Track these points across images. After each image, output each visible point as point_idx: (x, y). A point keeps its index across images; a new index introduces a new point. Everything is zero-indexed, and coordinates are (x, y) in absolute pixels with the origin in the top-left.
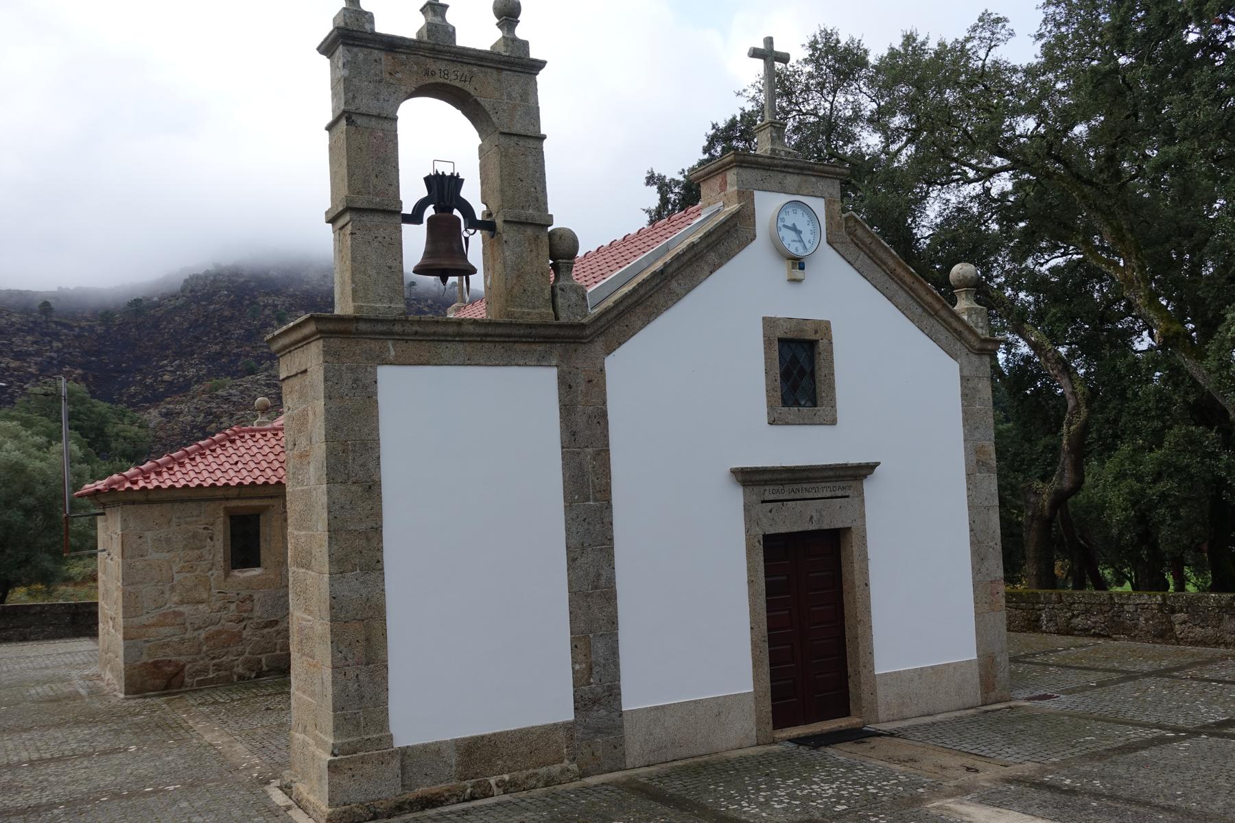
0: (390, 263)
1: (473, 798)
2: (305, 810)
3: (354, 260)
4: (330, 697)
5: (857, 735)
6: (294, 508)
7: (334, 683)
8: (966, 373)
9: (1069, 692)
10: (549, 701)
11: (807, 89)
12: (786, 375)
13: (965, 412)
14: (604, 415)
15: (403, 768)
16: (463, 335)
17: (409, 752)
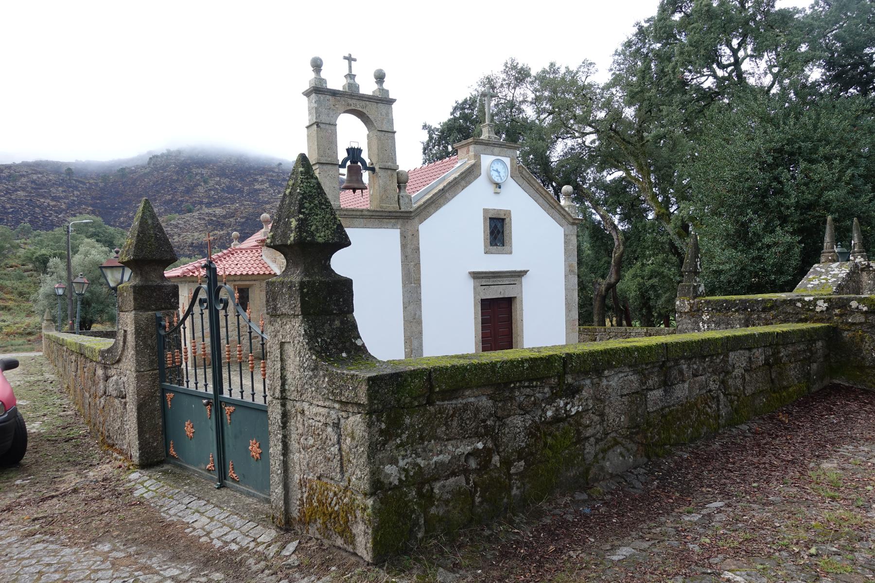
12: (492, 233)
14: (418, 249)
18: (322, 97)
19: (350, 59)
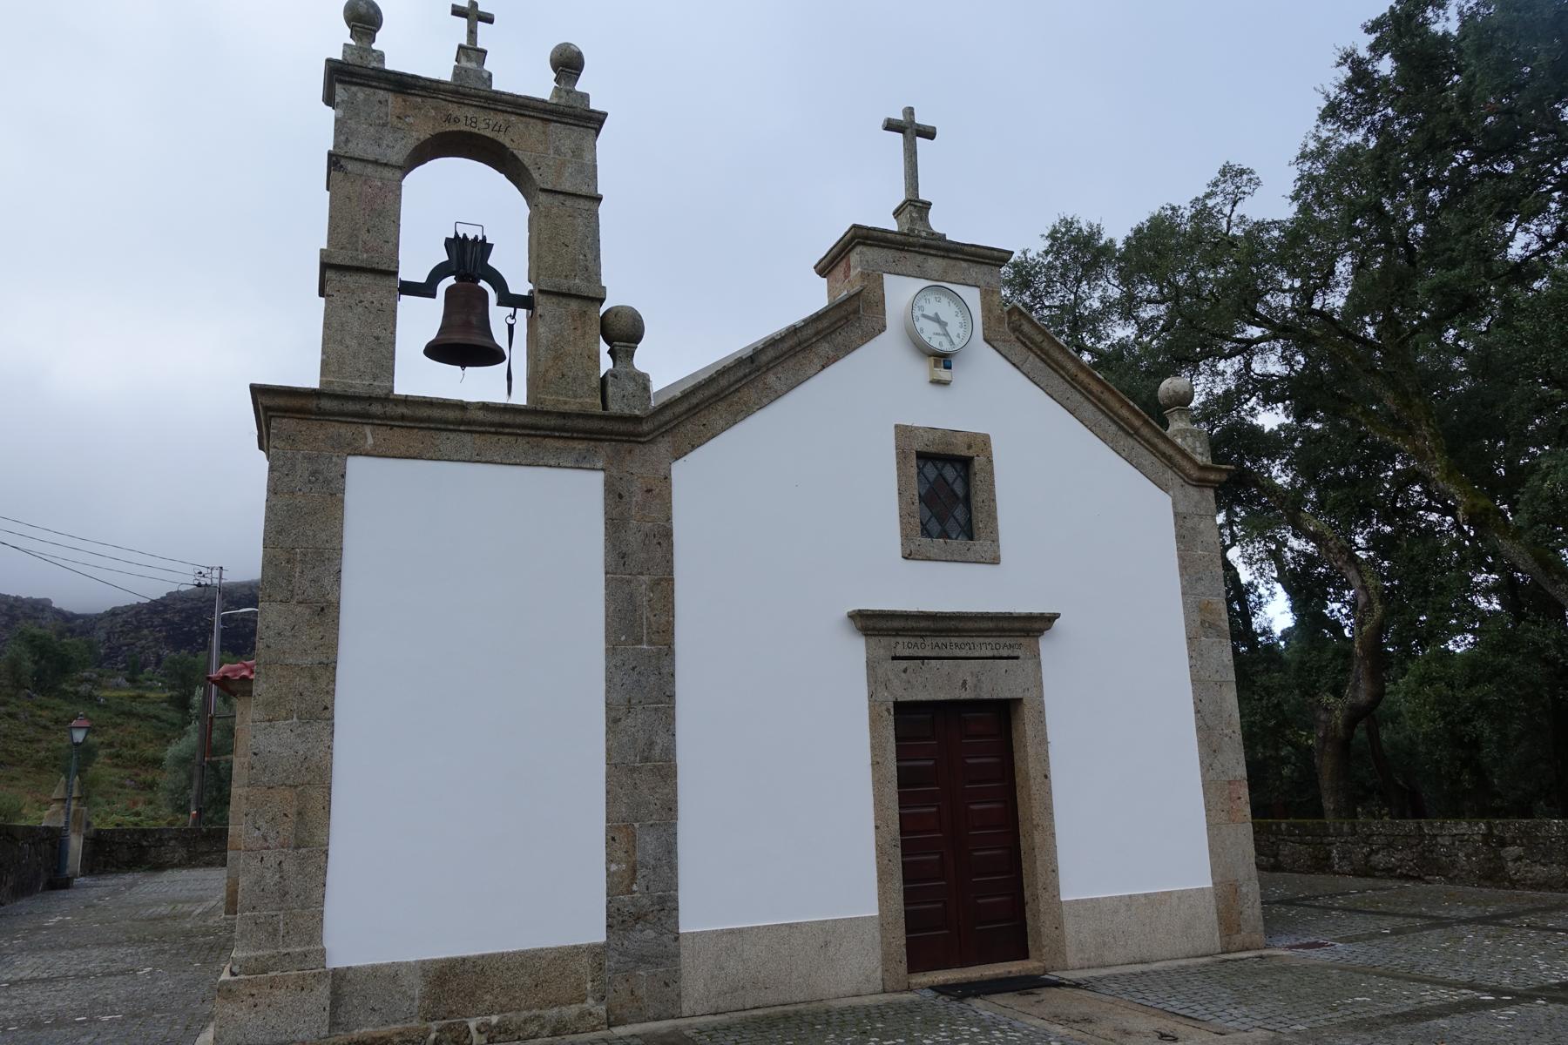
0: (377, 332)
5: (1028, 985)
8: (1181, 509)
9: (1348, 940)
10: (567, 909)
13: (1181, 558)
14: (668, 534)
16: (469, 423)
17: (350, 975)
18: (361, 94)
19: (473, 15)
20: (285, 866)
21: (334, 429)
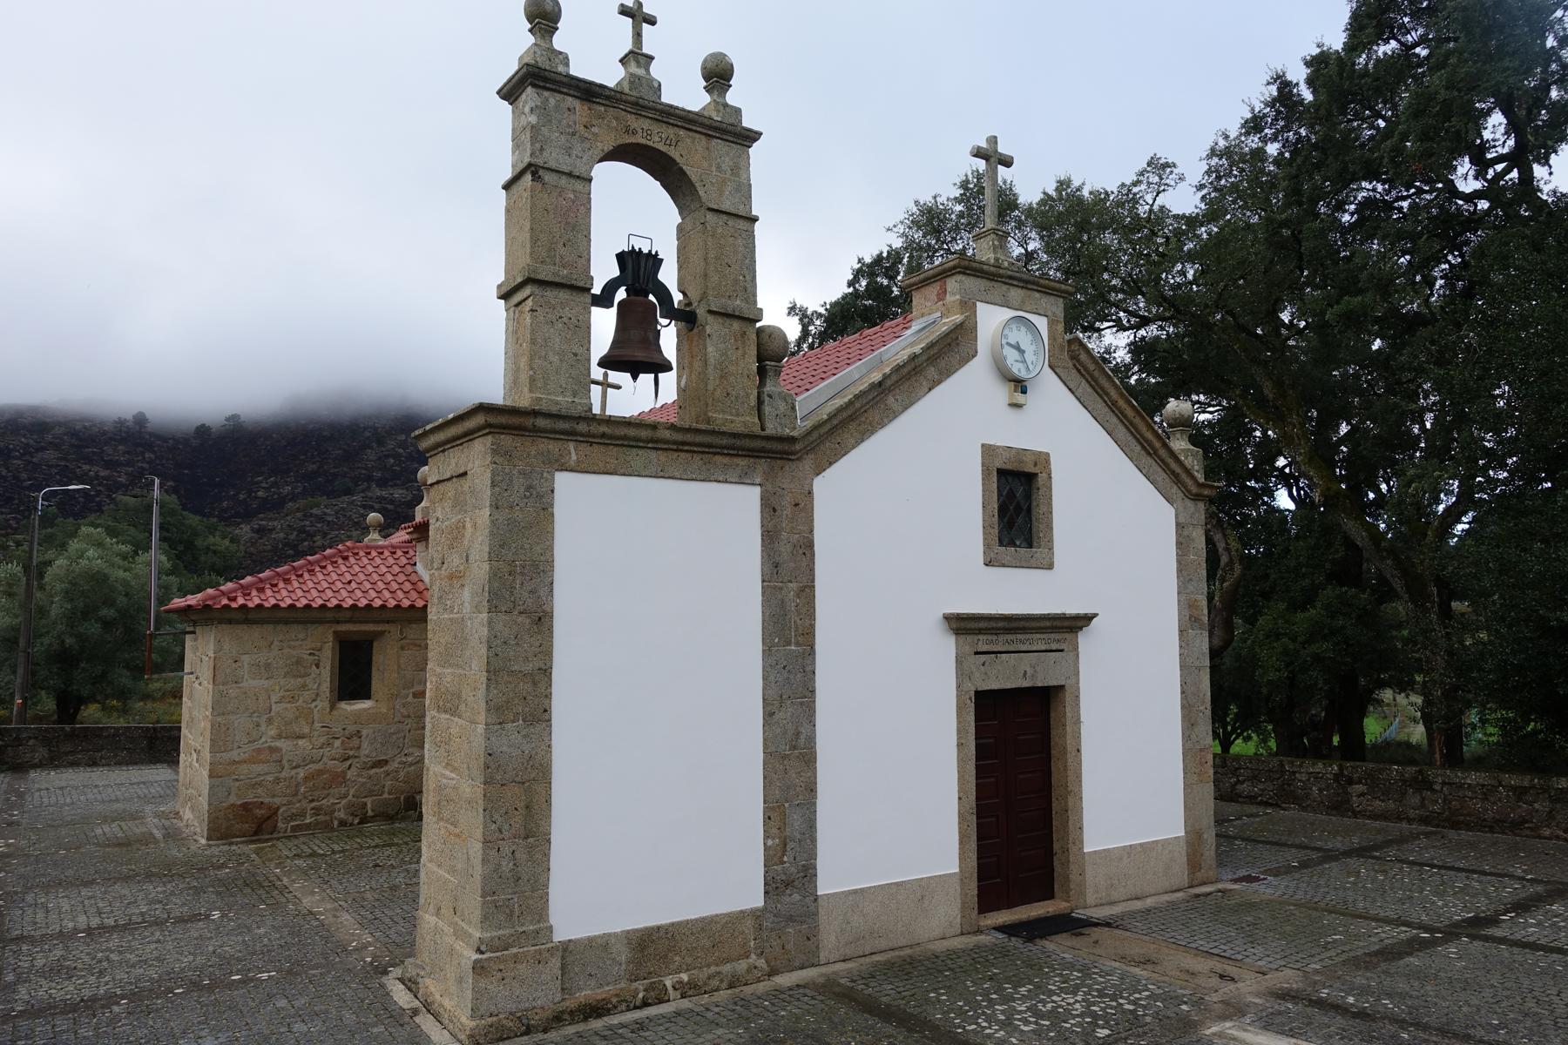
1: (645, 1004)
2: (436, 1016)
3: (533, 342)
4: (478, 878)
5: (1068, 924)
6: (437, 637)
7: (485, 861)
8: (1182, 520)
9: (1276, 873)
11: (957, 229)
12: (1002, 510)
13: (1179, 562)
14: (810, 545)
15: (563, 968)
16: (657, 441)
17: (571, 947)
18: (553, 99)
19: (638, 17)
20: (517, 855)
21: (545, 445)
